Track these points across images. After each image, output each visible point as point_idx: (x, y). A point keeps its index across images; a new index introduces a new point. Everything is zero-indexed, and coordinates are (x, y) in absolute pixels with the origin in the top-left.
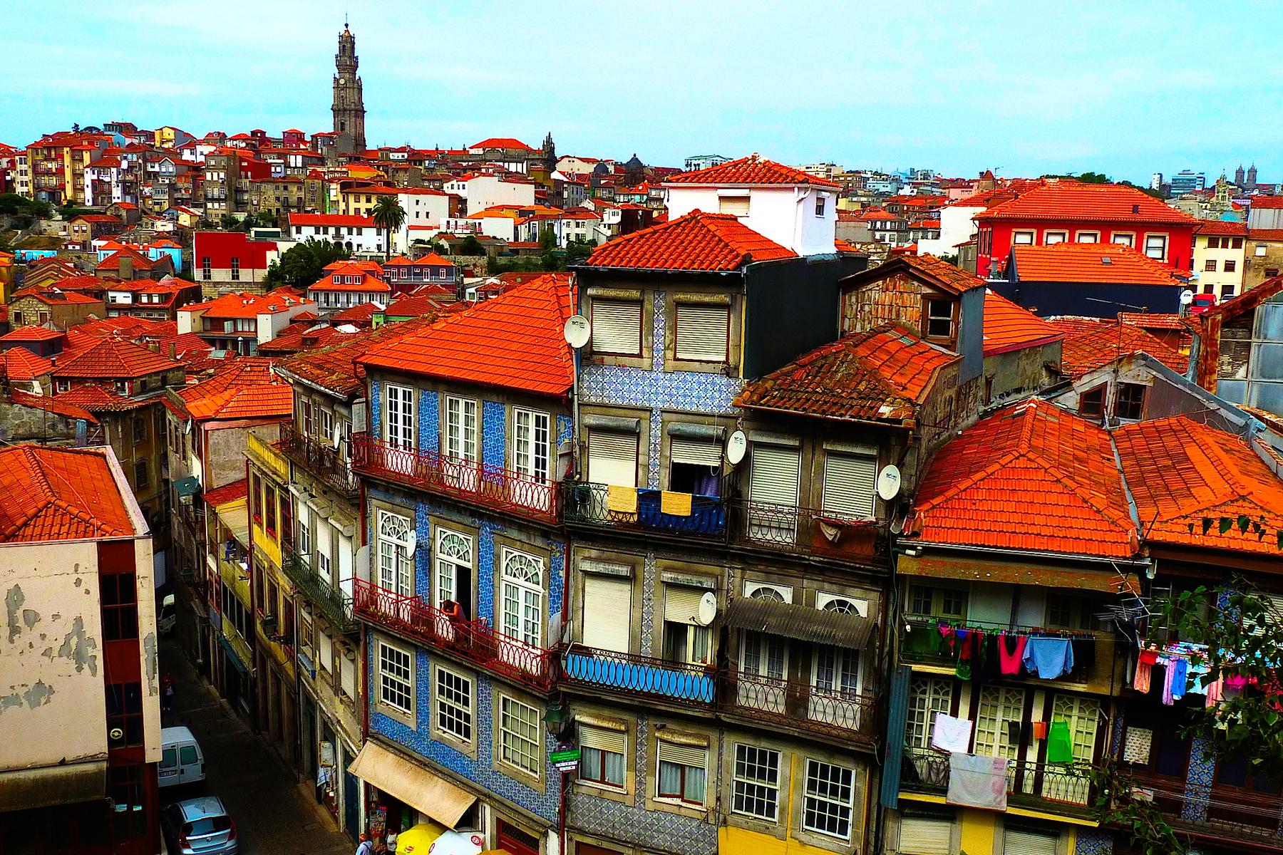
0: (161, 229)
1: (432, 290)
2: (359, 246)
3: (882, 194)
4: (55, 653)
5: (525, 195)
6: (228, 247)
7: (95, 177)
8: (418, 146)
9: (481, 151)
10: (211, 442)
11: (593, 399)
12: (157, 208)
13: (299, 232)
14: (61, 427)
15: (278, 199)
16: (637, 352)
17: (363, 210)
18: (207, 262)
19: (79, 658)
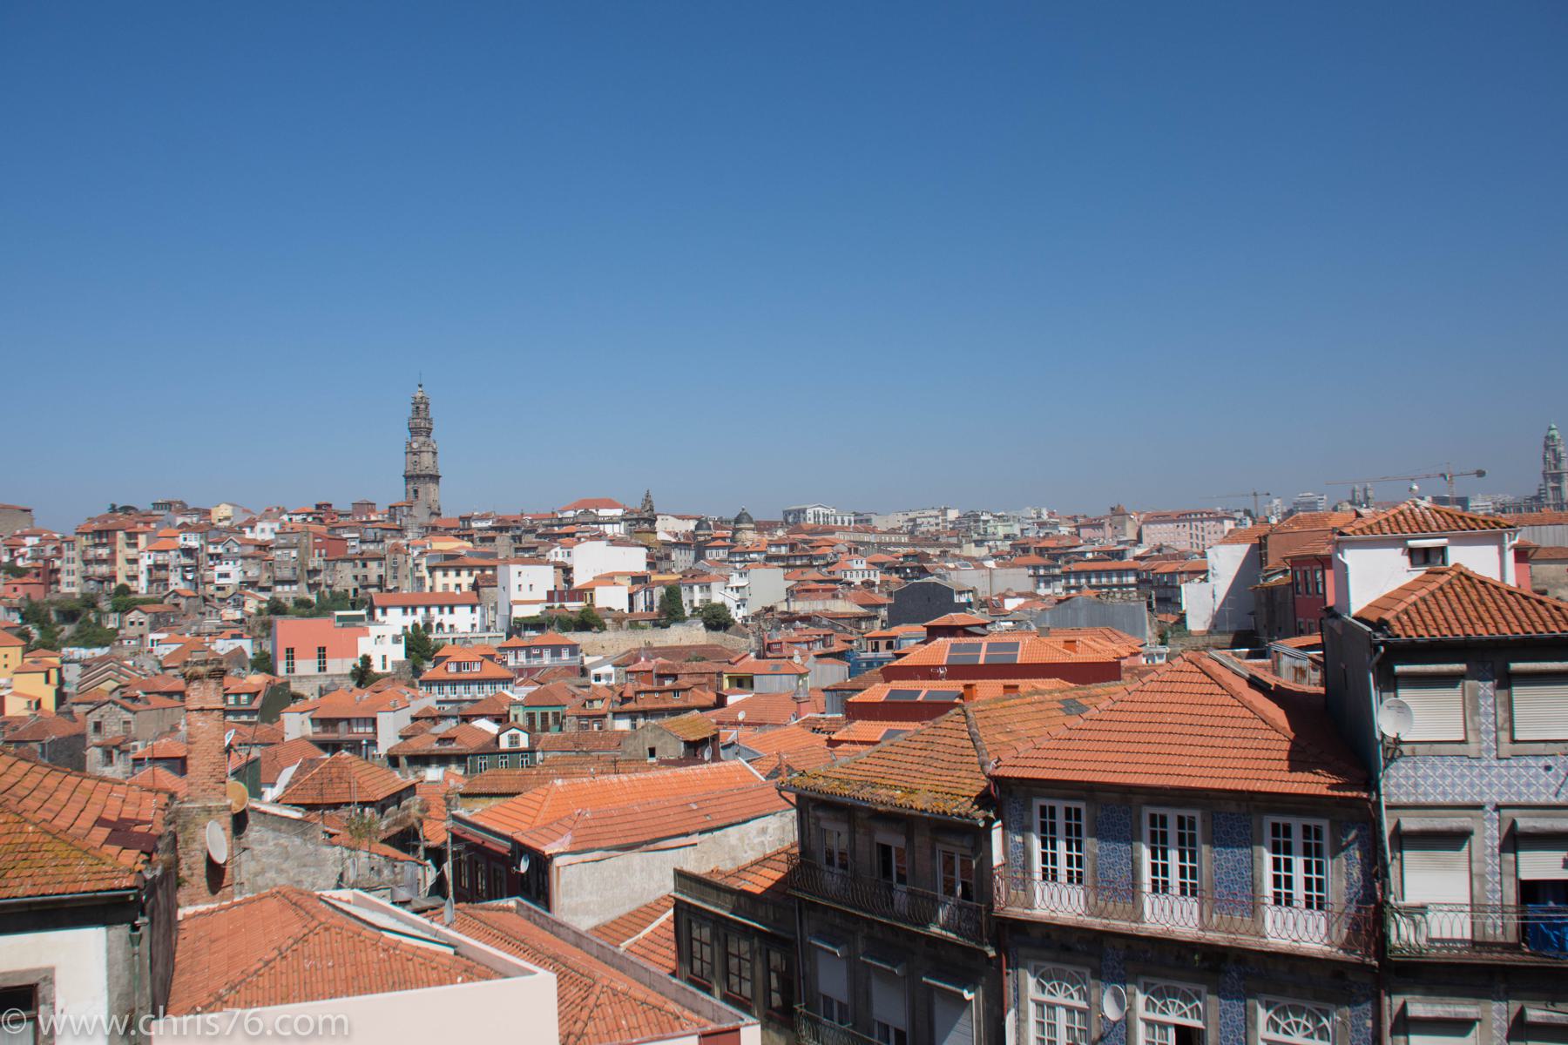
1: (554, 672)
2: (452, 626)
3: (1007, 537)
5: (636, 559)
7: (151, 562)
8: (502, 513)
9: (571, 514)
10: (562, 881)
11: (1404, 800)
12: (220, 594)
13: (384, 612)
14: (386, 872)
15: (356, 577)
16: (1461, 738)
17: (452, 589)
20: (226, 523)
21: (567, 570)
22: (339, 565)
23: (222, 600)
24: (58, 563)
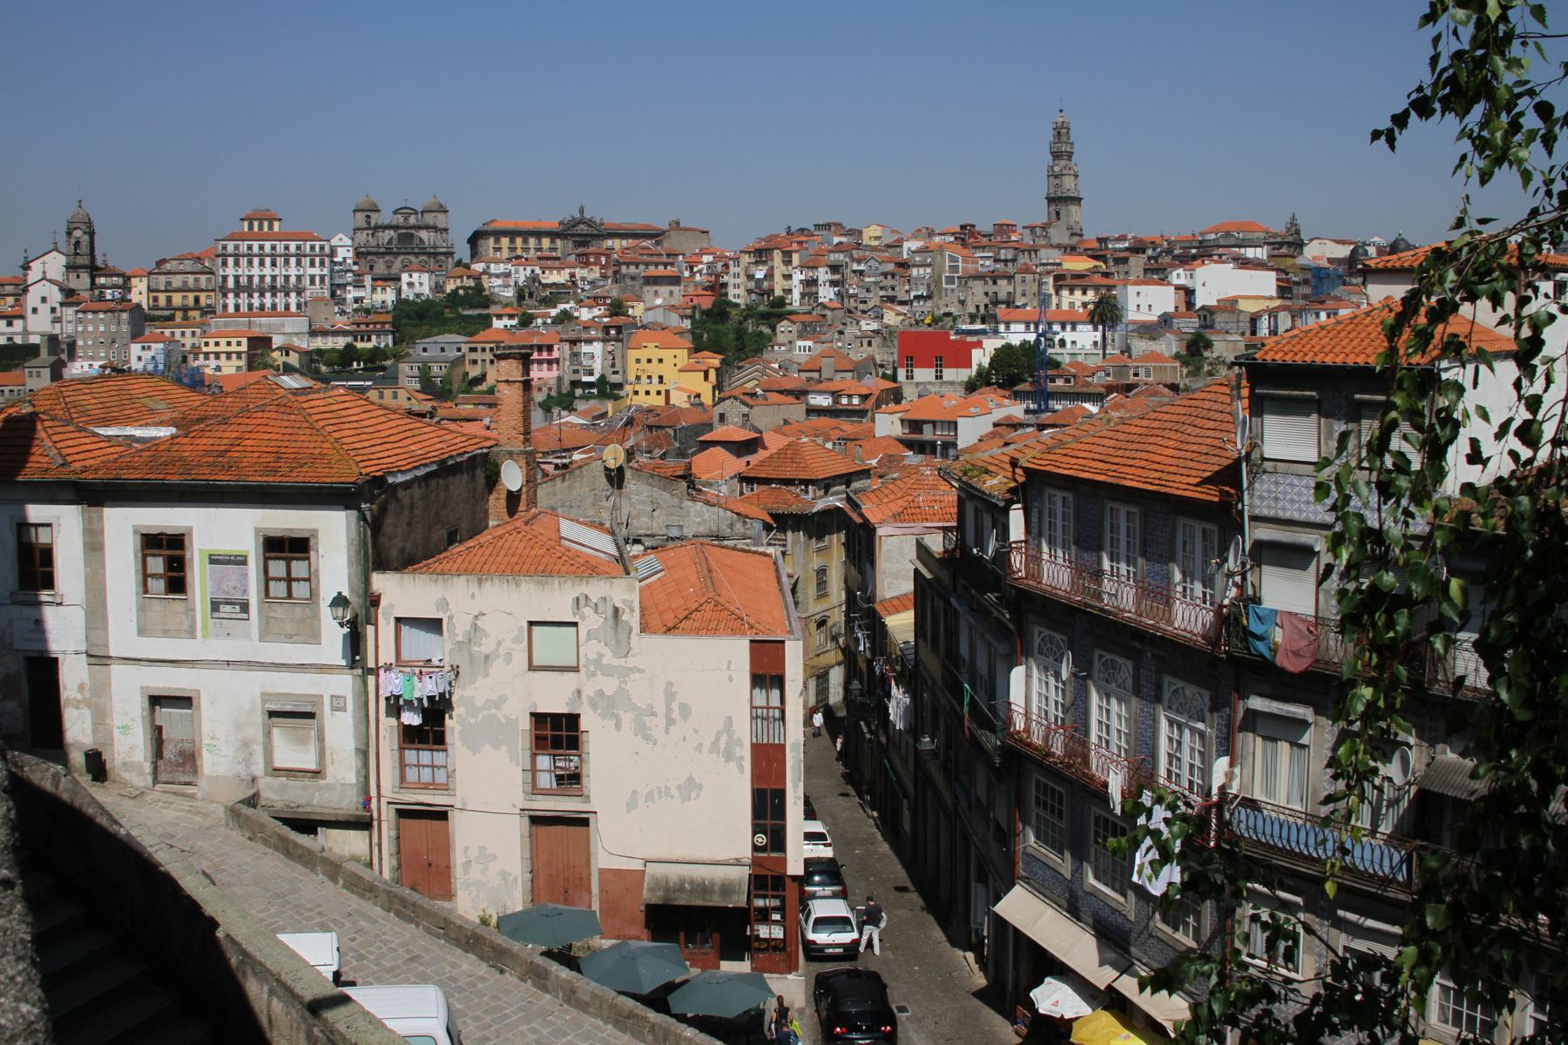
0: (864, 328)
2: (1074, 342)
4: (706, 747)
6: (932, 346)
10: (884, 549)
13: (1008, 328)
14: (739, 528)
15: (986, 294)
18: (910, 361)
19: (729, 756)
20: (875, 243)
21: (1189, 293)
22: (970, 283)
23: (864, 312)
24: (726, 278)
